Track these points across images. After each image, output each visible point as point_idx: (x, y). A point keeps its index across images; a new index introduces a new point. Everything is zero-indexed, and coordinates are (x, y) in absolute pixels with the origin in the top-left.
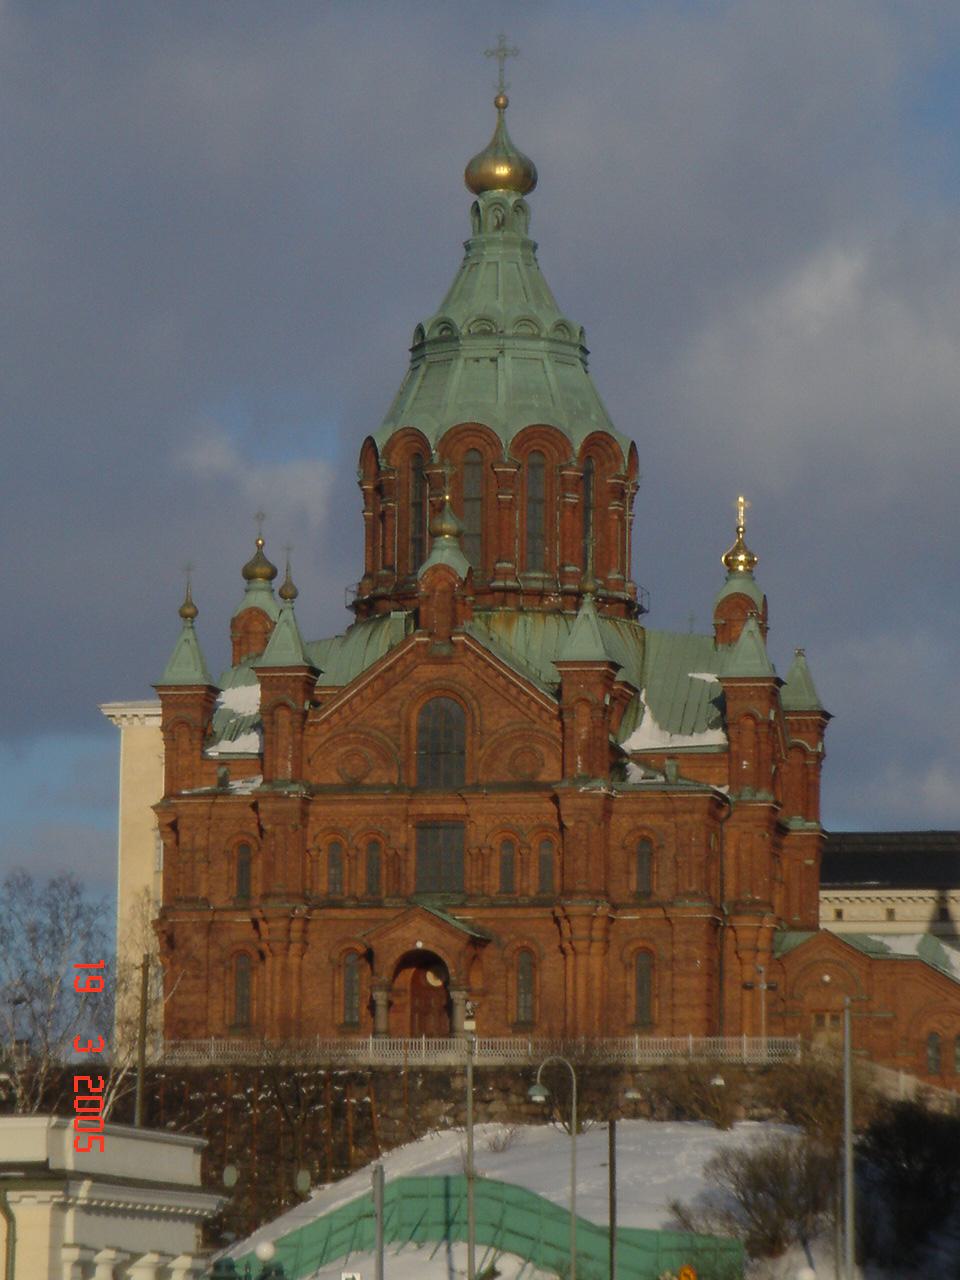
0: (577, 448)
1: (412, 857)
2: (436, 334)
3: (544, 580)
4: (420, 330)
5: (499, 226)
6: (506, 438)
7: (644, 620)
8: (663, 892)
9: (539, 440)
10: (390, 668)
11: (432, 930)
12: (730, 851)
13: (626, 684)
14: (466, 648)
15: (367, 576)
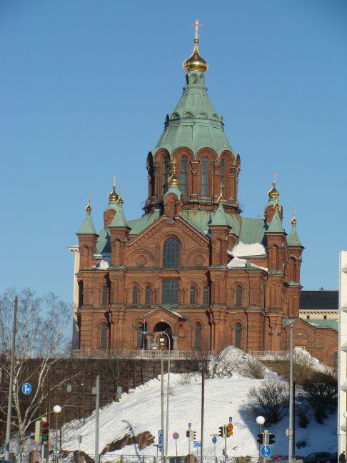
0: (219, 156)
1: (161, 291)
2: (173, 118)
3: (207, 200)
4: (168, 117)
5: (195, 82)
6: (195, 152)
7: (241, 214)
8: (245, 304)
9: (207, 152)
10: (154, 228)
11: (166, 316)
12: (268, 290)
13: (234, 235)
14: (180, 221)
15: (148, 199)
